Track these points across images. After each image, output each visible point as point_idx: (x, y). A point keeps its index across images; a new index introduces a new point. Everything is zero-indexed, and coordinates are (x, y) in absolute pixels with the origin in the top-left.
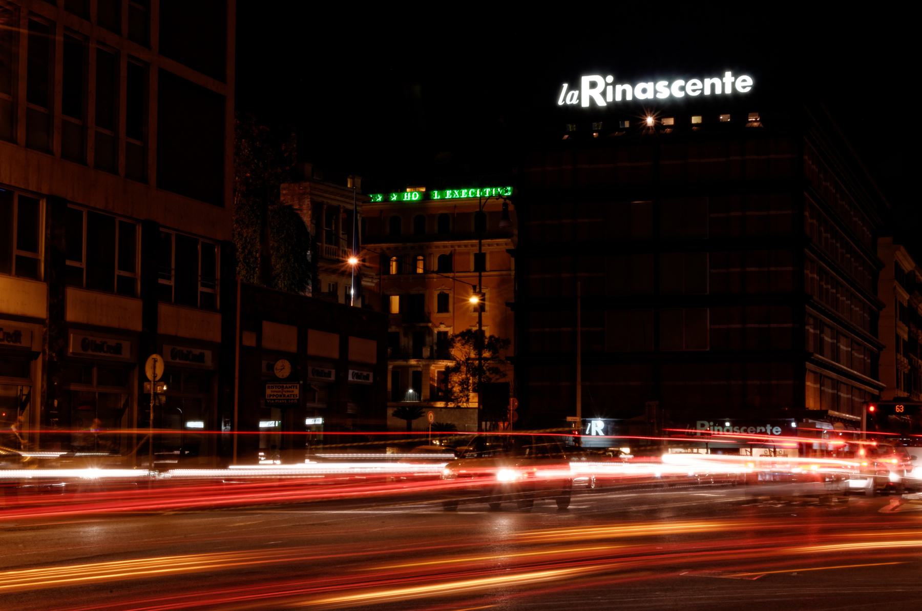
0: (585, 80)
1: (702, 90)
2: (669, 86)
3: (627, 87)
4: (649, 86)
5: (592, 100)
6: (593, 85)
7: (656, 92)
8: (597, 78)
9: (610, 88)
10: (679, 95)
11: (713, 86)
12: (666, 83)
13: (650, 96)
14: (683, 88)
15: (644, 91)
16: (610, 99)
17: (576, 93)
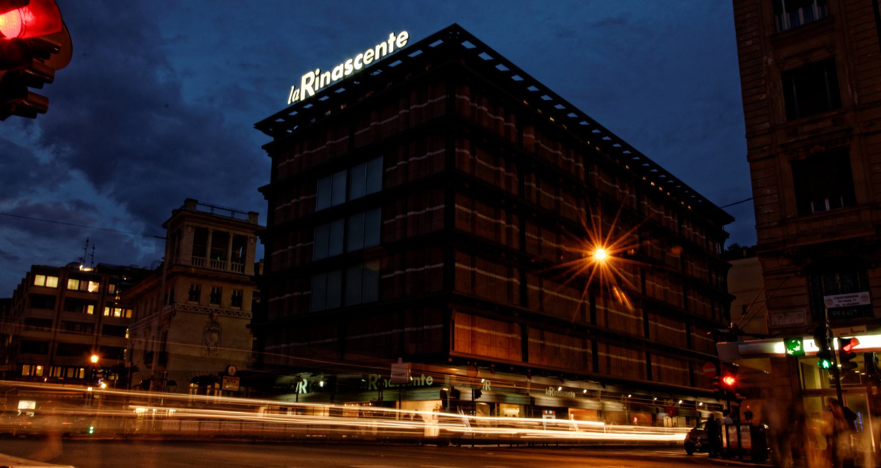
0: (304, 78)
1: (374, 57)
2: (353, 63)
3: (328, 74)
4: (340, 68)
5: (306, 92)
6: (308, 80)
7: (344, 70)
8: (311, 75)
9: (318, 78)
10: (359, 67)
11: (381, 50)
12: (350, 61)
13: (341, 76)
14: (361, 61)
15: (338, 73)
16: (317, 88)
17: (298, 91)
